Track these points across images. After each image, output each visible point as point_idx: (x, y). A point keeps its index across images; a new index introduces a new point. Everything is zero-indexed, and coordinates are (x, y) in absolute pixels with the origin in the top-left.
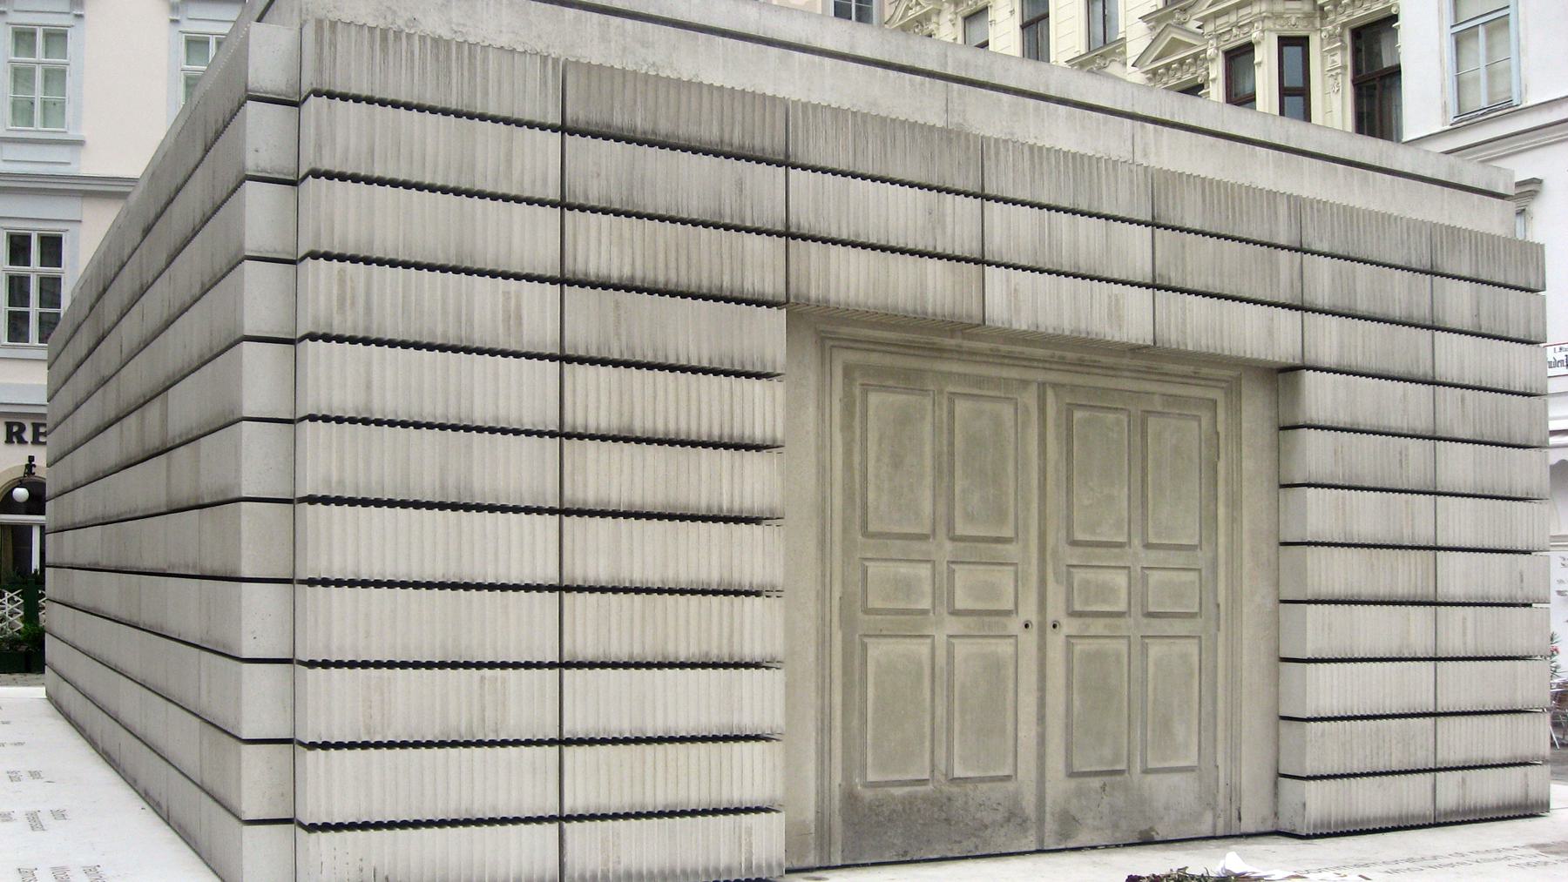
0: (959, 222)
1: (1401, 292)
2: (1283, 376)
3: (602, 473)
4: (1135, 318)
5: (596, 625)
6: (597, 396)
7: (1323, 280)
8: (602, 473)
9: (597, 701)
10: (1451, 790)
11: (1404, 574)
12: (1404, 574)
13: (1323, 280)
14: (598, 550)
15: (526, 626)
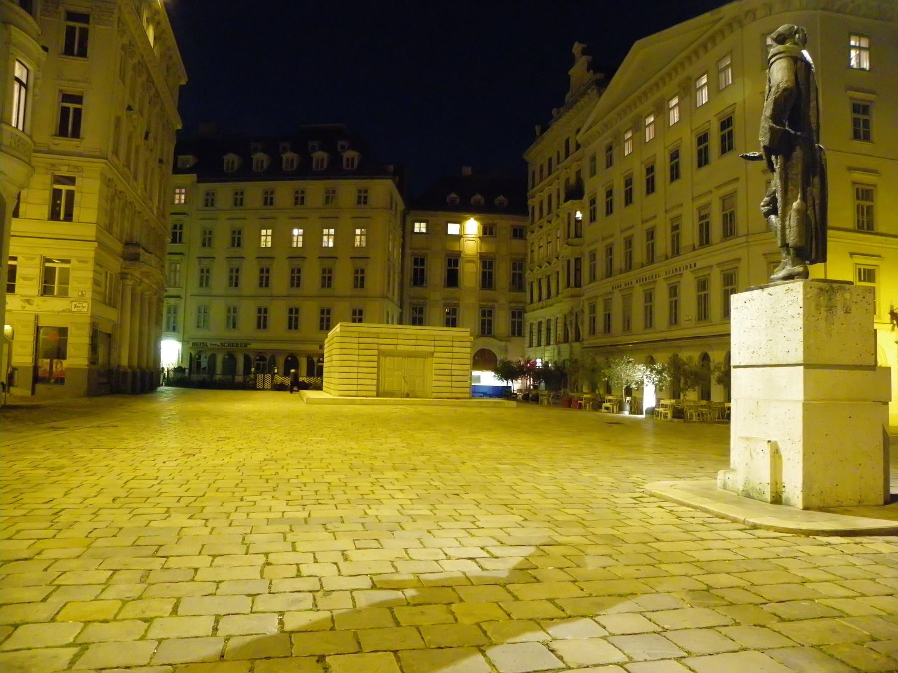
0: (395, 342)
1: (450, 344)
2: (432, 354)
3: (361, 364)
4: (413, 349)
5: (360, 376)
6: (361, 358)
7: (437, 343)
8: (361, 364)
9: (360, 382)
10: (453, 395)
11: (447, 372)
12: (447, 372)
13: (437, 343)
14: (361, 370)
15: (355, 376)
